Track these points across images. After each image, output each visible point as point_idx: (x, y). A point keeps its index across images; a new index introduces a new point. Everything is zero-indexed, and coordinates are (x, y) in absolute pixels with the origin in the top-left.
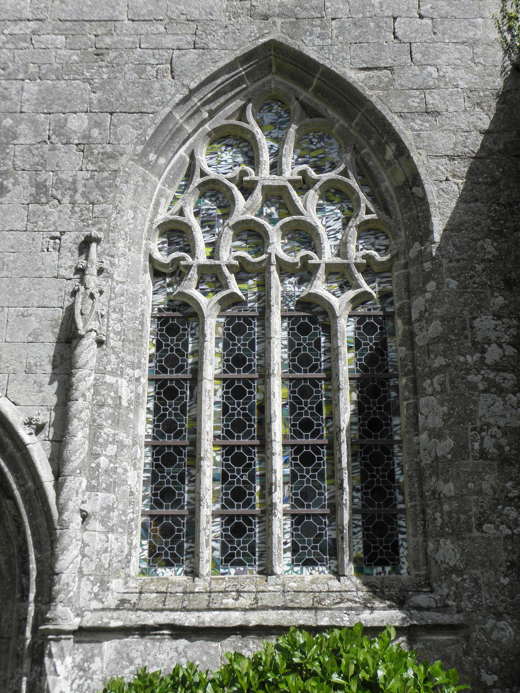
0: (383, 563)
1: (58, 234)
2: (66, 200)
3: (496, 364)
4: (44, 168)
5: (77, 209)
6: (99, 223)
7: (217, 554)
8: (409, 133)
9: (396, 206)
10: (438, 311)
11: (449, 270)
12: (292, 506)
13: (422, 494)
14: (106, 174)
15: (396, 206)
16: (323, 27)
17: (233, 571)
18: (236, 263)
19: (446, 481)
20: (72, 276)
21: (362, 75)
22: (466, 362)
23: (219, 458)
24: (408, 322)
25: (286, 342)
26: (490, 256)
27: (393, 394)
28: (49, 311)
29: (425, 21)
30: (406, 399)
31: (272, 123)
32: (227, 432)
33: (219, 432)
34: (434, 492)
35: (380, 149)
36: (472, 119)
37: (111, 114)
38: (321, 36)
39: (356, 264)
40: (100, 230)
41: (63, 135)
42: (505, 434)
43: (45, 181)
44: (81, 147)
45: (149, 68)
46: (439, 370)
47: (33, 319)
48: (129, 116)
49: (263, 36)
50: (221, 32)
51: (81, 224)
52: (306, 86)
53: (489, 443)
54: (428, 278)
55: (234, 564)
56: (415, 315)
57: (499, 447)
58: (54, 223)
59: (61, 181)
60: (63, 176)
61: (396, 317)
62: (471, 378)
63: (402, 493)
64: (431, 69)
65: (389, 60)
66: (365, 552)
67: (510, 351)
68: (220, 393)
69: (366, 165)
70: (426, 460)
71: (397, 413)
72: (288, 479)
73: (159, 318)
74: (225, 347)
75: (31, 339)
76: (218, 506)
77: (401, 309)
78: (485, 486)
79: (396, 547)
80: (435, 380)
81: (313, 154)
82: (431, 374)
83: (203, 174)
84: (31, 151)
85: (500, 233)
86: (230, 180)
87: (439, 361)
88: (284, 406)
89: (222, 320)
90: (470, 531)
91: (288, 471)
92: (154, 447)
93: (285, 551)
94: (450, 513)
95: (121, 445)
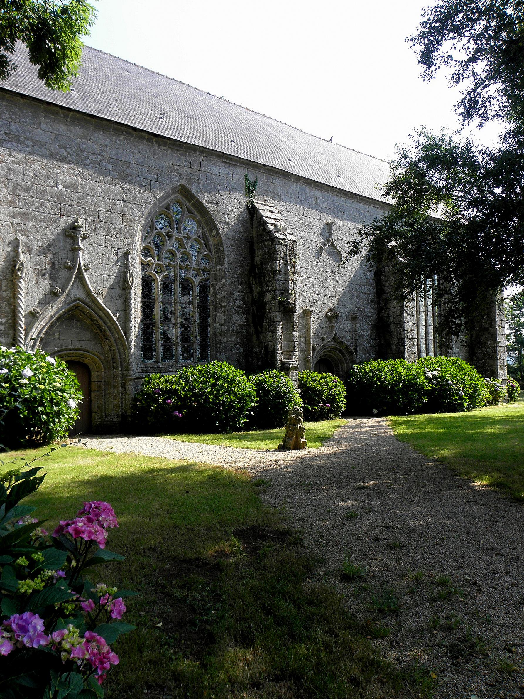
0: (204, 359)
2: (118, 236)
8: (221, 228)
9: (213, 251)
10: (225, 289)
11: (229, 276)
13: (216, 341)
15: (213, 251)
16: (199, 184)
19: (224, 338)
21: (209, 205)
24: (214, 289)
34: (220, 340)
35: (211, 231)
36: (238, 227)
37: (131, 203)
38: (198, 187)
46: (224, 306)
50: (166, 177)
52: (189, 202)
54: (223, 277)
55: (167, 359)
56: (217, 288)
62: (232, 309)
67: (241, 302)
69: (205, 234)
71: (209, 317)
77: (212, 285)
78: (233, 340)
82: (221, 307)
83: (156, 229)
85: (241, 266)
94: (224, 347)
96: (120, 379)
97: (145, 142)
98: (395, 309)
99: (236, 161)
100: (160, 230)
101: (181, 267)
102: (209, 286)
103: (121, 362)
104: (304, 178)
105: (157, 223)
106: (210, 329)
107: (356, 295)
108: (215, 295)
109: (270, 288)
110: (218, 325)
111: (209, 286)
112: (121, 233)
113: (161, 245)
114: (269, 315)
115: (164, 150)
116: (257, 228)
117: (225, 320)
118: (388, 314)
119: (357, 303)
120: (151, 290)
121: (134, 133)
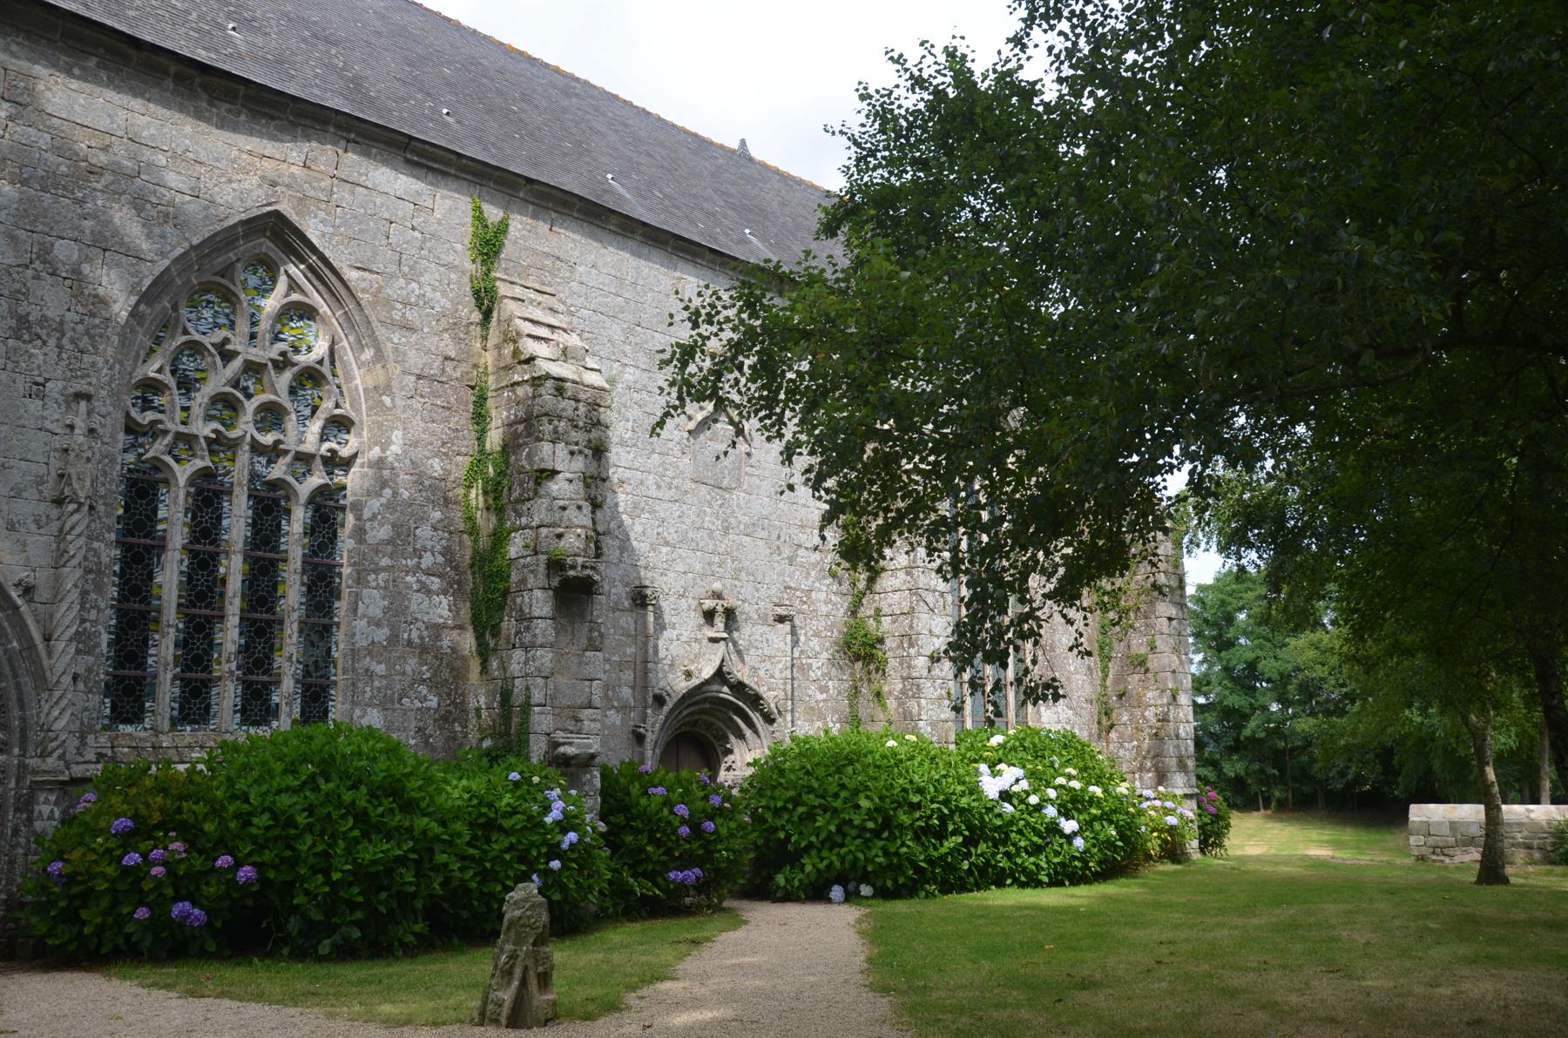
1: (40, 380)
2: (52, 342)
3: (429, 568)
4: (27, 299)
5: (64, 356)
6: (88, 376)
7: (175, 713)
12: (244, 674)
14: (97, 321)
17: (188, 728)
18: (213, 436)
20: (59, 431)
22: (407, 566)
23: (181, 626)
24: (359, 518)
25: (250, 521)
26: (436, 474)
27: (337, 580)
28: (33, 466)
29: (417, 234)
30: (348, 587)
31: (255, 288)
32: (191, 601)
33: (183, 601)
34: (367, 670)
37: (105, 250)
39: (322, 456)
40: (90, 384)
41: (49, 263)
42: (427, 628)
43: (28, 314)
44: (68, 282)
45: (148, 206)
46: (384, 569)
47: (15, 471)
48: (124, 258)
49: (269, 204)
51: (69, 374)
53: (415, 635)
55: (190, 723)
56: (367, 514)
57: (421, 638)
58: (39, 367)
59: (44, 318)
60: (49, 314)
61: (348, 510)
62: (409, 579)
63: (335, 667)
64: (414, 285)
65: (381, 266)
66: (301, 716)
67: (440, 559)
68: (186, 563)
70: (362, 643)
72: (243, 649)
73: (128, 479)
74: (193, 518)
75: (12, 494)
76: (178, 670)
78: (408, 669)
79: (326, 712)
80: (380, 577)
81: (293, 333)
82: (376, 571)
83: (185, 332)
84: (10, 275)
86: (213, 345)
87: (385, 562)
88: (243, 581)
89: (192, 490)
90: (392, 702)
91: (243, 641)
92: (119, 610)
93: (235, 712)
95: (99, 610)
96: (12, 784)
97: (169, 83)
98: (897, 596)
99: (448, 163)
100: (197, 337)
101: (257, 448)
102: (343, 509)
103: (23, 730)
104: (644, 224)
105: (193, 316)
106: (340, 636)
107: (787, 552)
108: (359, 533)
109: (524, 520)
110: (364, 622)
111: (343, 509)
112: (63, 335)
113: (197, 380)
114: (519, 600)
115: (229, 111)
116: (498, 347)
117: (386, 610)
118: (878, 610)
119: (791, 576)
120: (155, 510)
121: (132, 52)
